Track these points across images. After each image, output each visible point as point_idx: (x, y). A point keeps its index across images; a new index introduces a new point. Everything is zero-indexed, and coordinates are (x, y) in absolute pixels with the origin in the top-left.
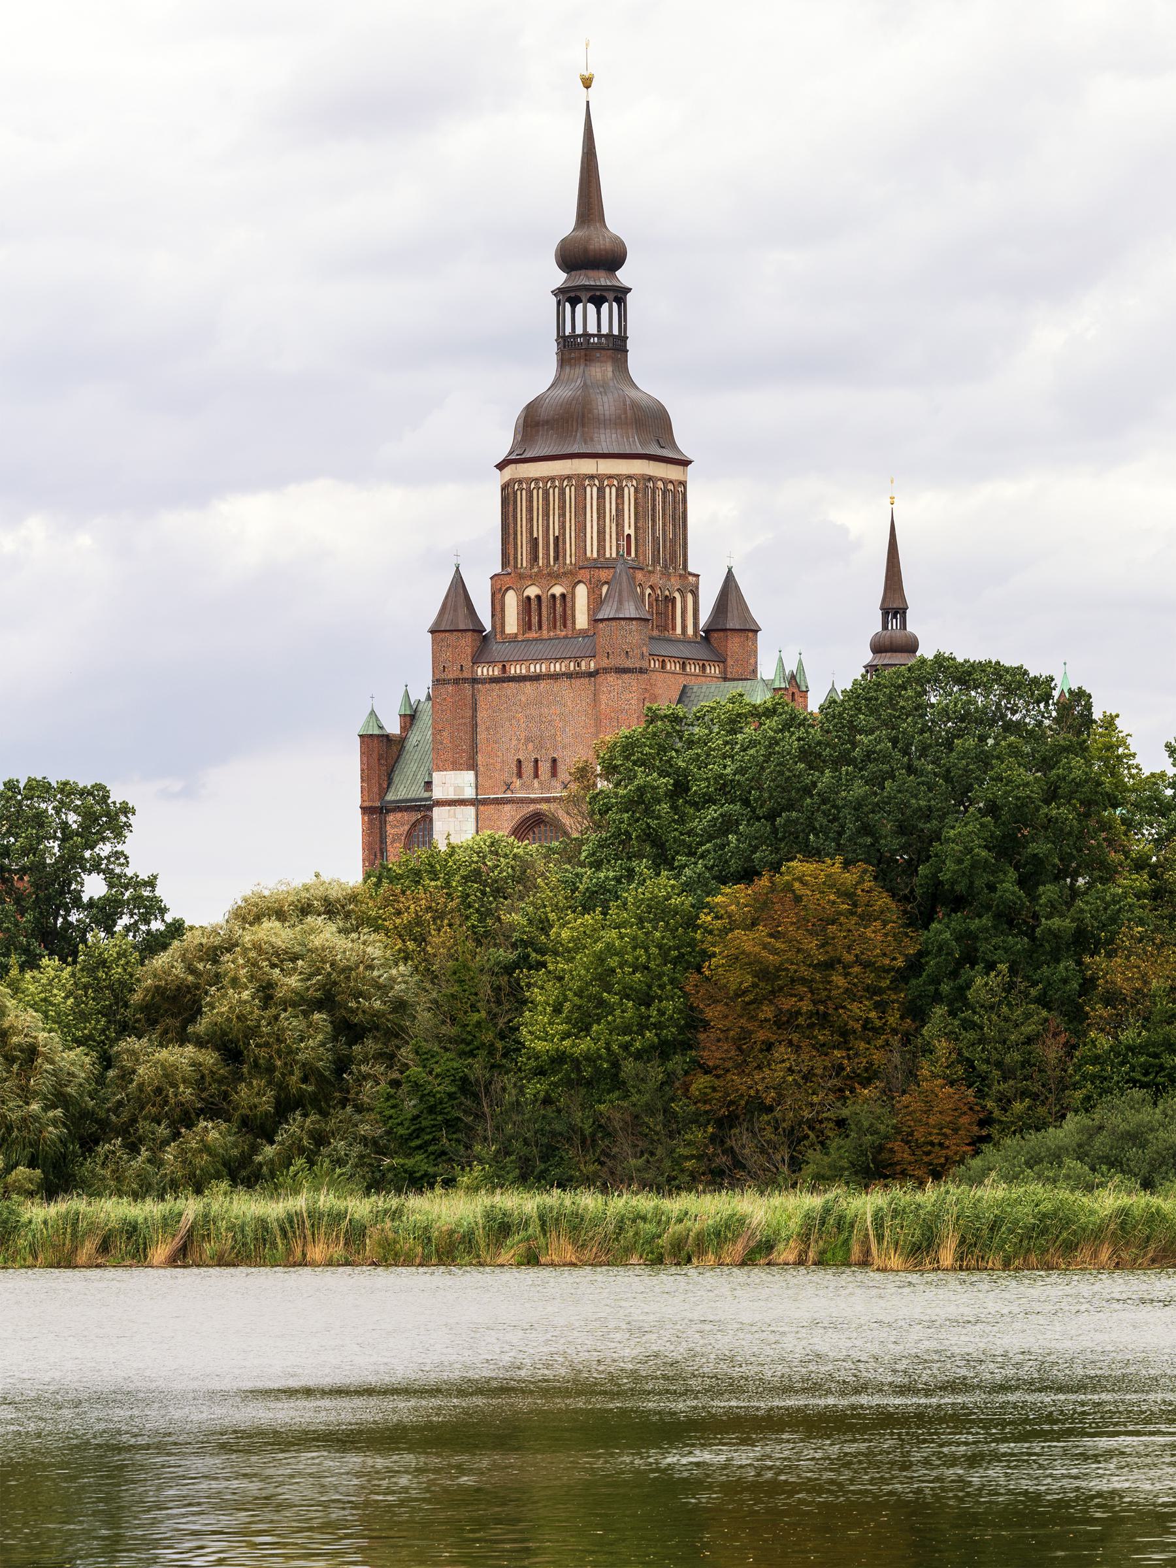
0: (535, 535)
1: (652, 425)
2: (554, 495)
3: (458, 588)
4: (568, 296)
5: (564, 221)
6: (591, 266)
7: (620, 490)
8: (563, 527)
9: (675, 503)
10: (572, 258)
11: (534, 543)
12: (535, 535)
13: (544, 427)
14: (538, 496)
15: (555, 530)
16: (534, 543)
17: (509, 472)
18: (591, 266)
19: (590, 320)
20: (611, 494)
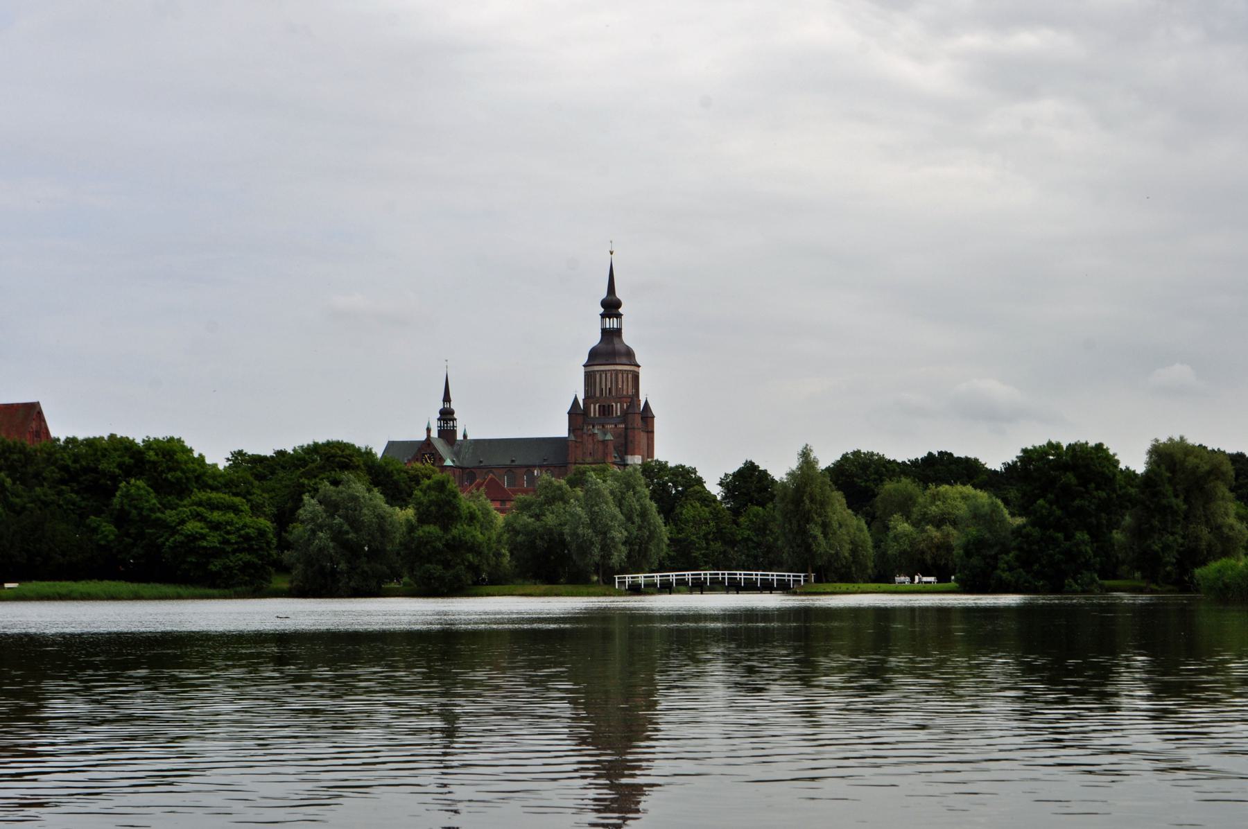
1: (629, 354)
3: (576, 400)
4: (603, 316)
5: (603, 294)
6: (611, 307)
9: (636, 378)
11: (601, 390)
13: (594, 355)
16: (601, 390)
18: (611, 307)
19: (611, 323)
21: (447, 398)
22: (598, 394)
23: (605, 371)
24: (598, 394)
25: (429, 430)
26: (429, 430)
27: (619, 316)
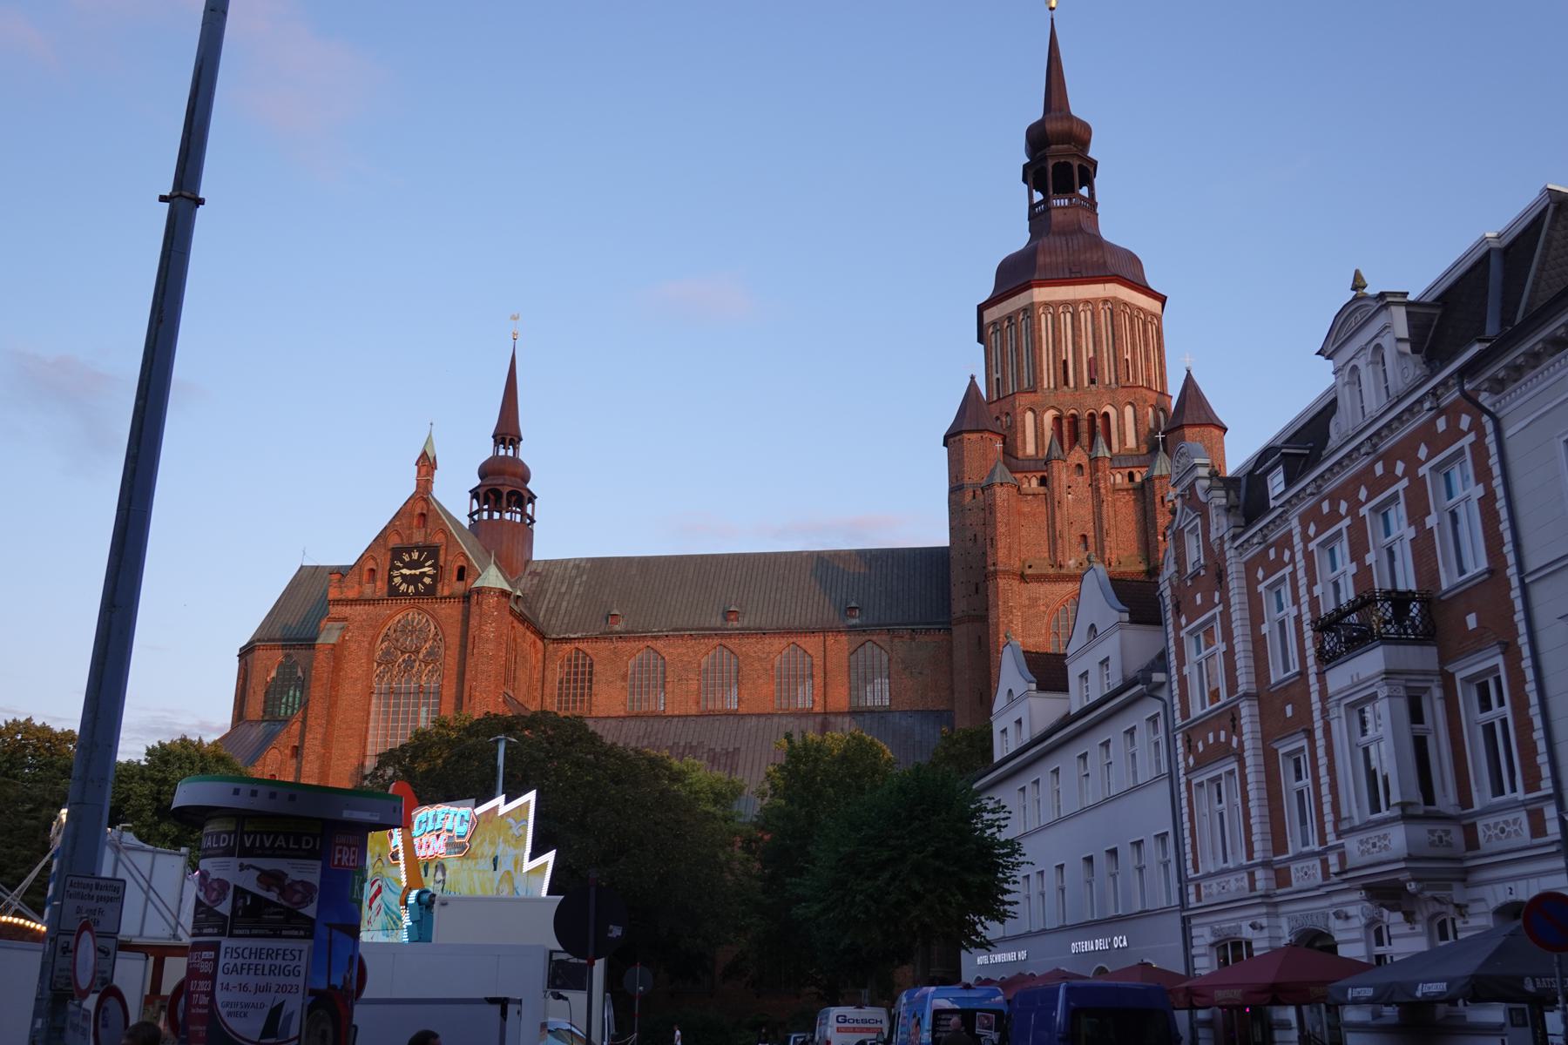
2: (1085, 317)
10: (1037, 139)
11: (1065, 362)
15: (1087, 352)
17: (991, 315)
20: (1138, 325)
21: (507, 434)
22: (1048, 380)
23: (1074, 303)
24: (1048, 380)
25: (427, 464)
26: (427, 464)
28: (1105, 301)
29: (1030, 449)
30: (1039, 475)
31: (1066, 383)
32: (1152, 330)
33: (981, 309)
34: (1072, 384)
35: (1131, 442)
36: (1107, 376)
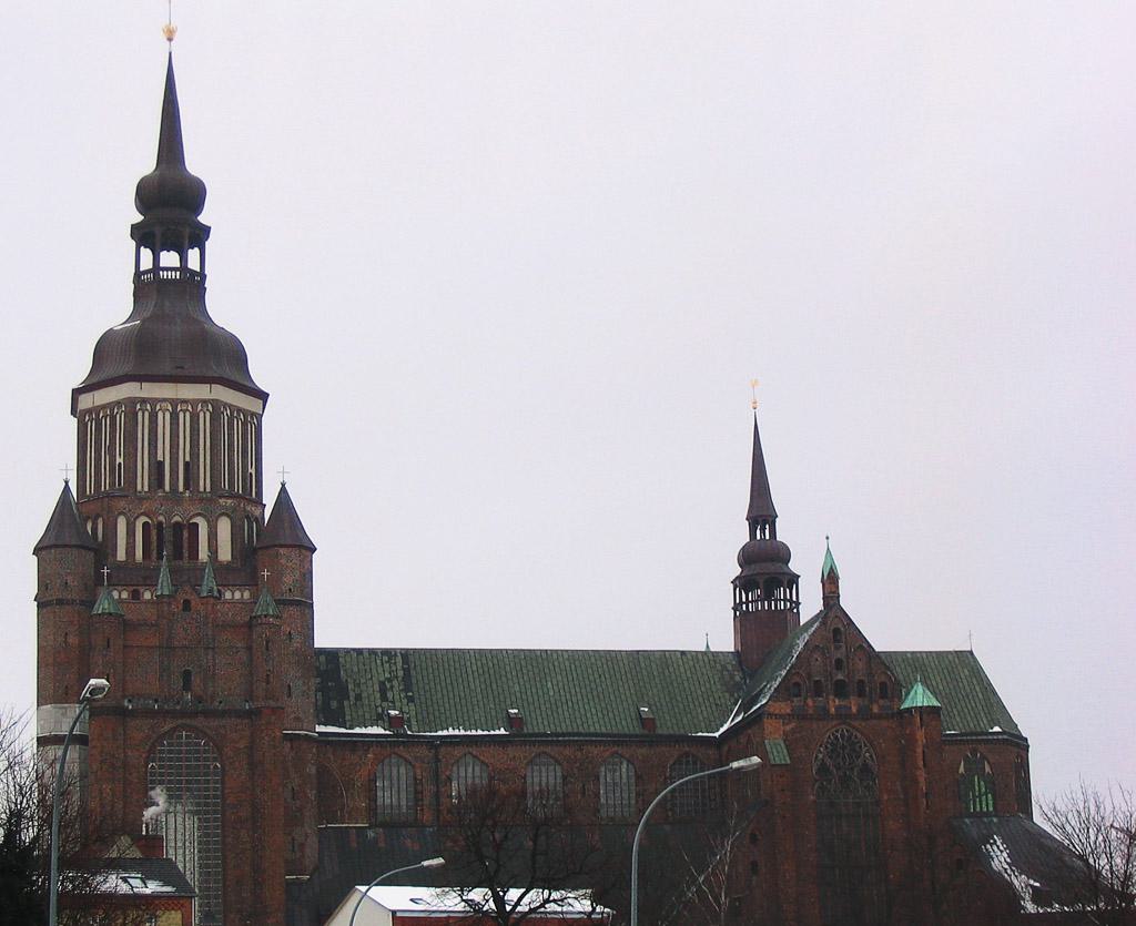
0: (160, 458)
4: (141, 235)
7: (244, 424)
8: (194, 454)
10: (148, 195)
11: (161, 464)
12: (160, 458)
13: (117, 357)
14: (164, 420)
15: (184, 455)
16: (157, 467)
17: (86, 401)
22: (143, 483)
24: (143, 483)
27: (199, 236)
28: (205, 402)
29: (121, 555)
30: (132, 588)
31: (161, 484)
32: (251, 429)
33: (76, 393)
34: (167, 488)
35: (225, 554)
36: (204, 483)
